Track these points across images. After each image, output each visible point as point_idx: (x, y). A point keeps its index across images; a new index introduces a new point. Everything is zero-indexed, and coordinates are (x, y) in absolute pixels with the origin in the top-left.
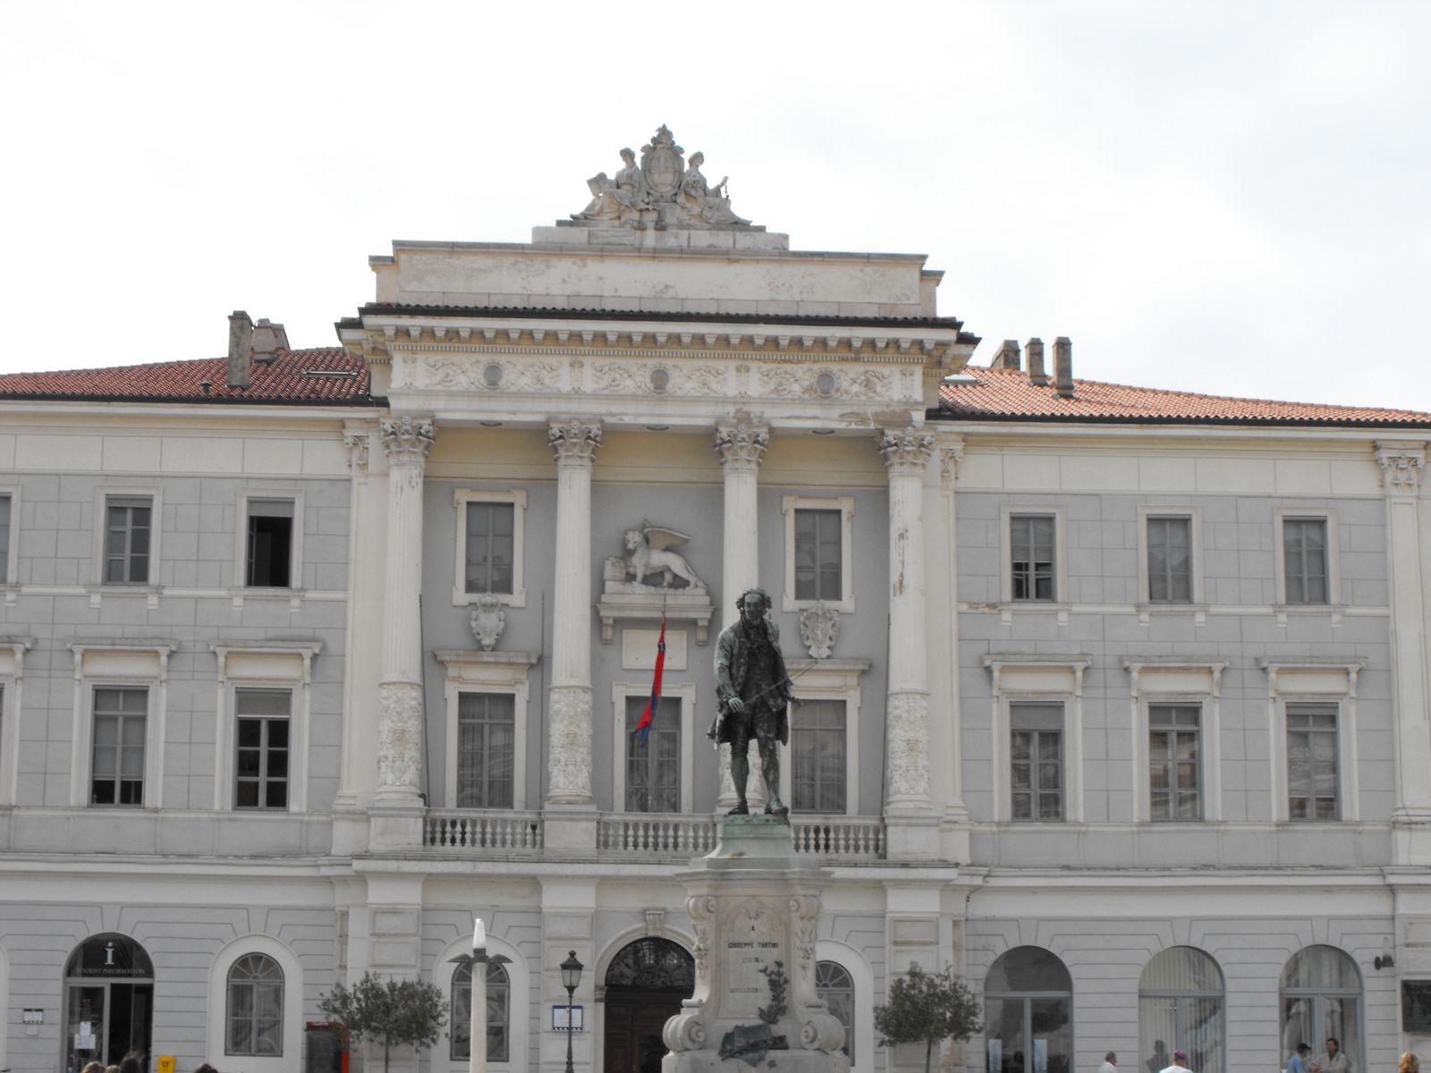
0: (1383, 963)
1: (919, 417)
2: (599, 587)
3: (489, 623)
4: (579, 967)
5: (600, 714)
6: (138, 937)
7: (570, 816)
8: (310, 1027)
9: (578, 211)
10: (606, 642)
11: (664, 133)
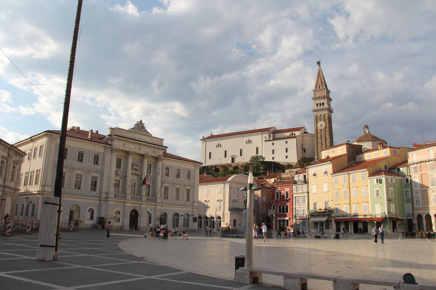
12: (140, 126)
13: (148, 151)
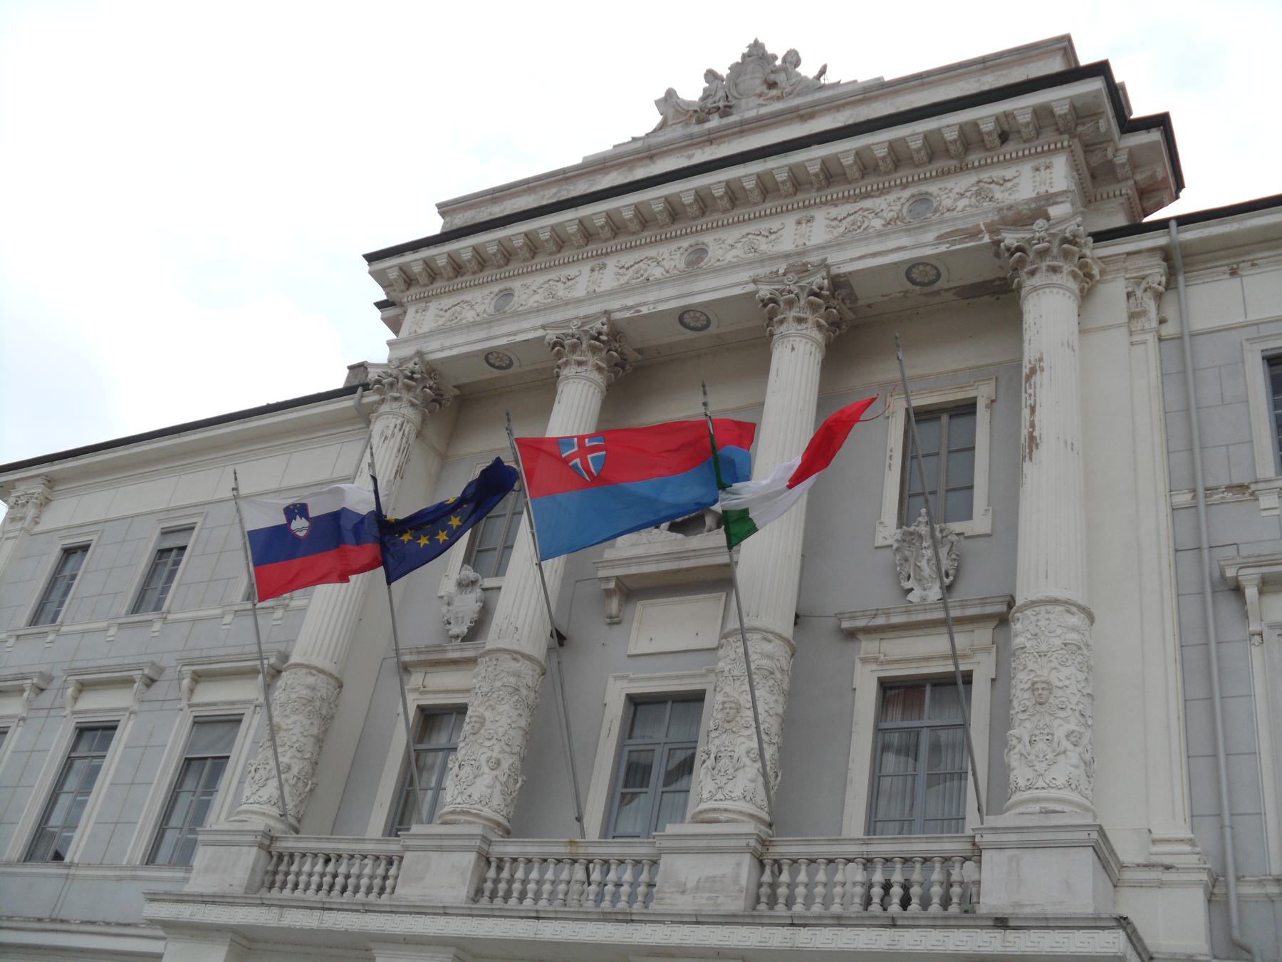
7: (437, 842)
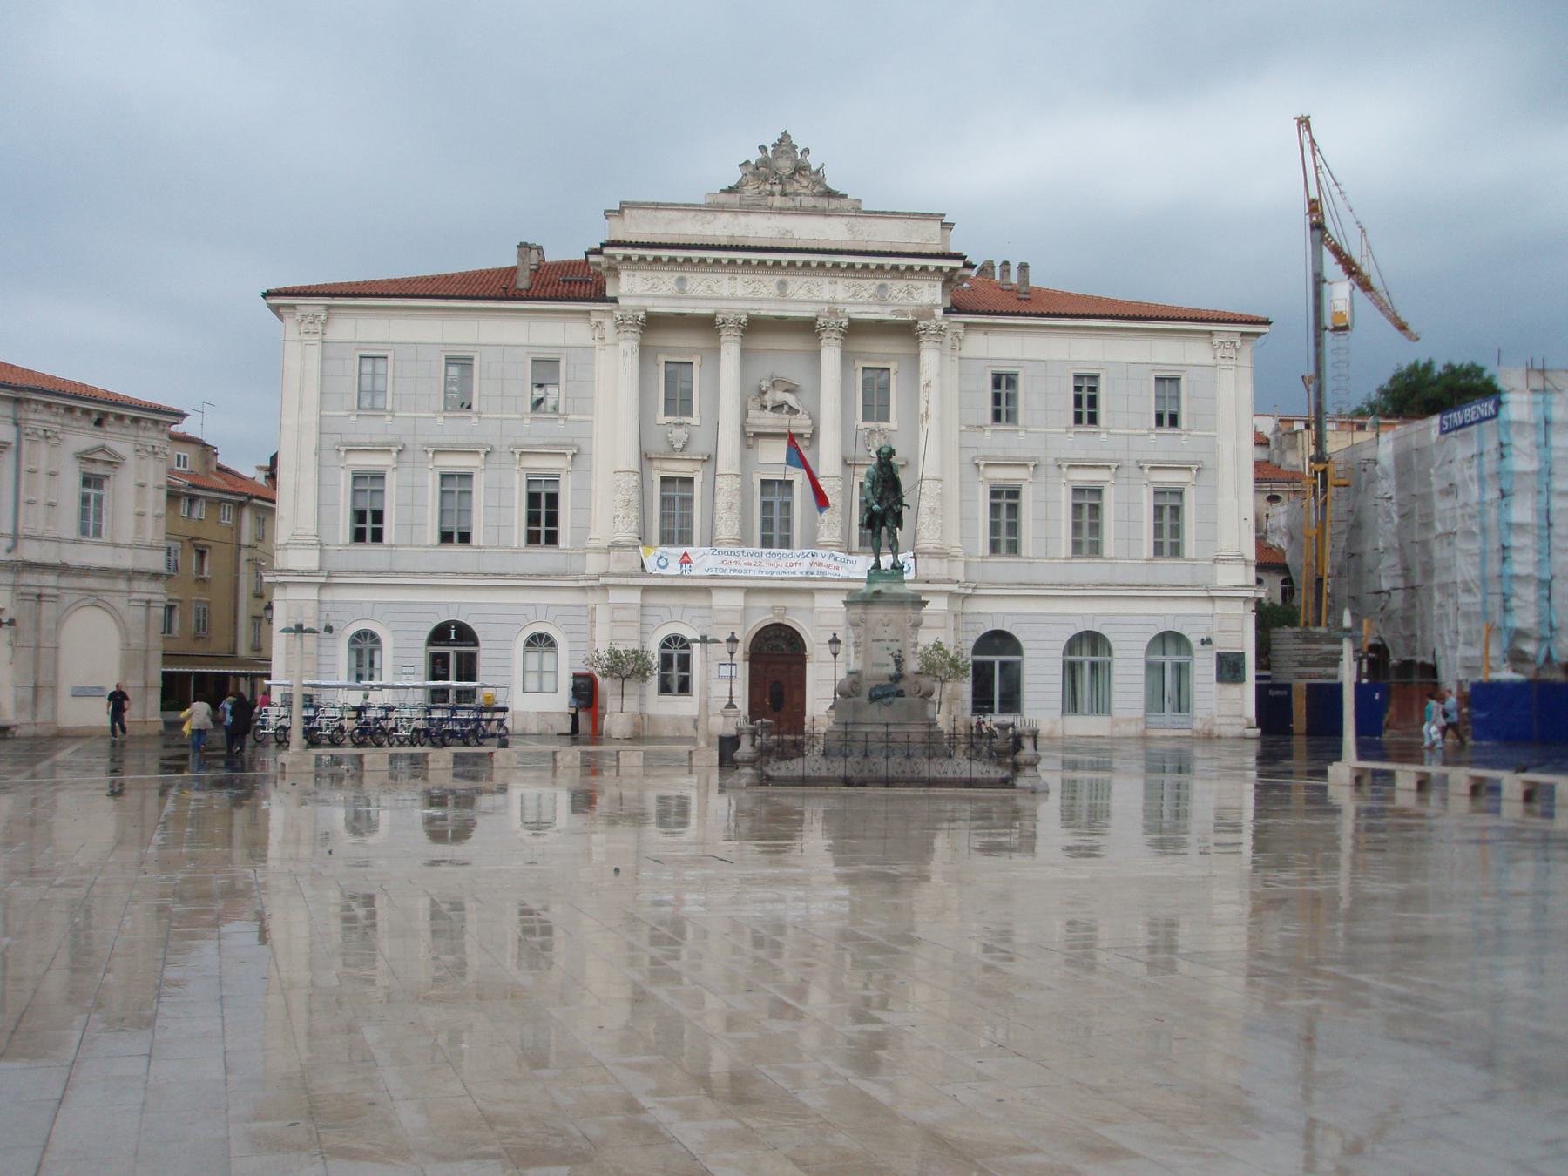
0: (1206, 642)
1: (939, 313)
2: (745, 413)
3: (679, 435)
4: (737, 641)
5: (745, 492)
6: (469, 623)
8: (576, 676)
9: (732, 184)
10: (749, 447)
11: (785, 134)
12: (782, 174)
13: (841, 296)
